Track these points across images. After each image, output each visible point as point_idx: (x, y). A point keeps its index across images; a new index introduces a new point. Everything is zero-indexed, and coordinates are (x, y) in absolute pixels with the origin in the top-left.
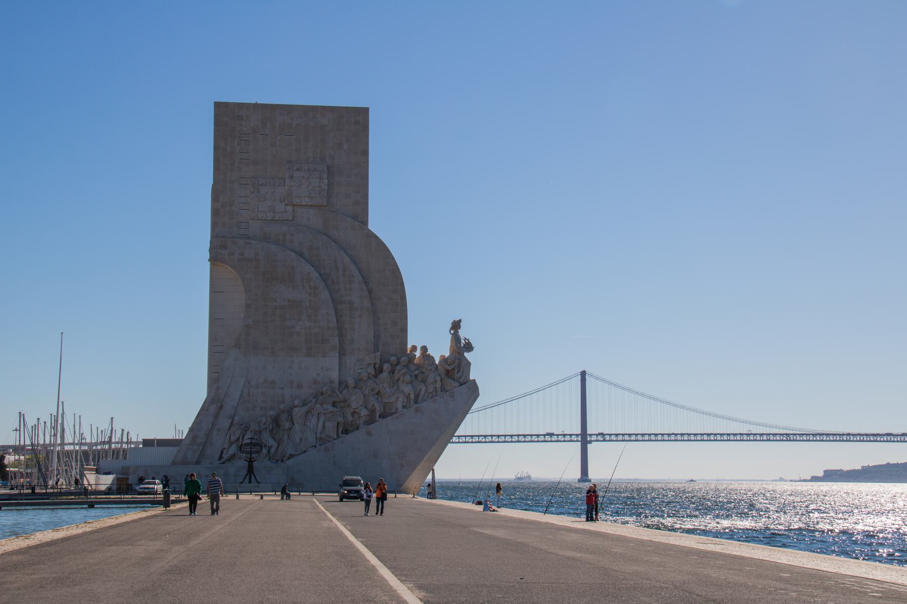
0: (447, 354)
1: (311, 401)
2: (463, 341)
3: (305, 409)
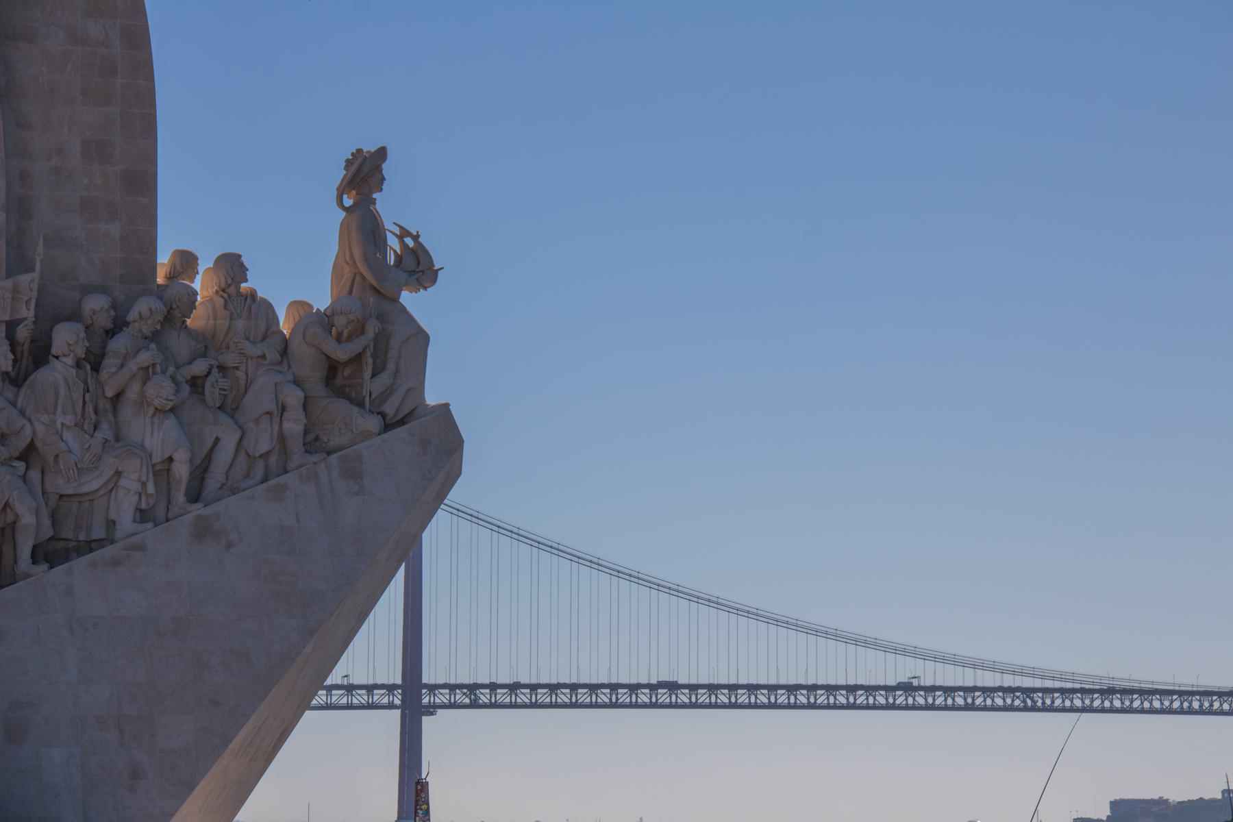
2: (393, 243)
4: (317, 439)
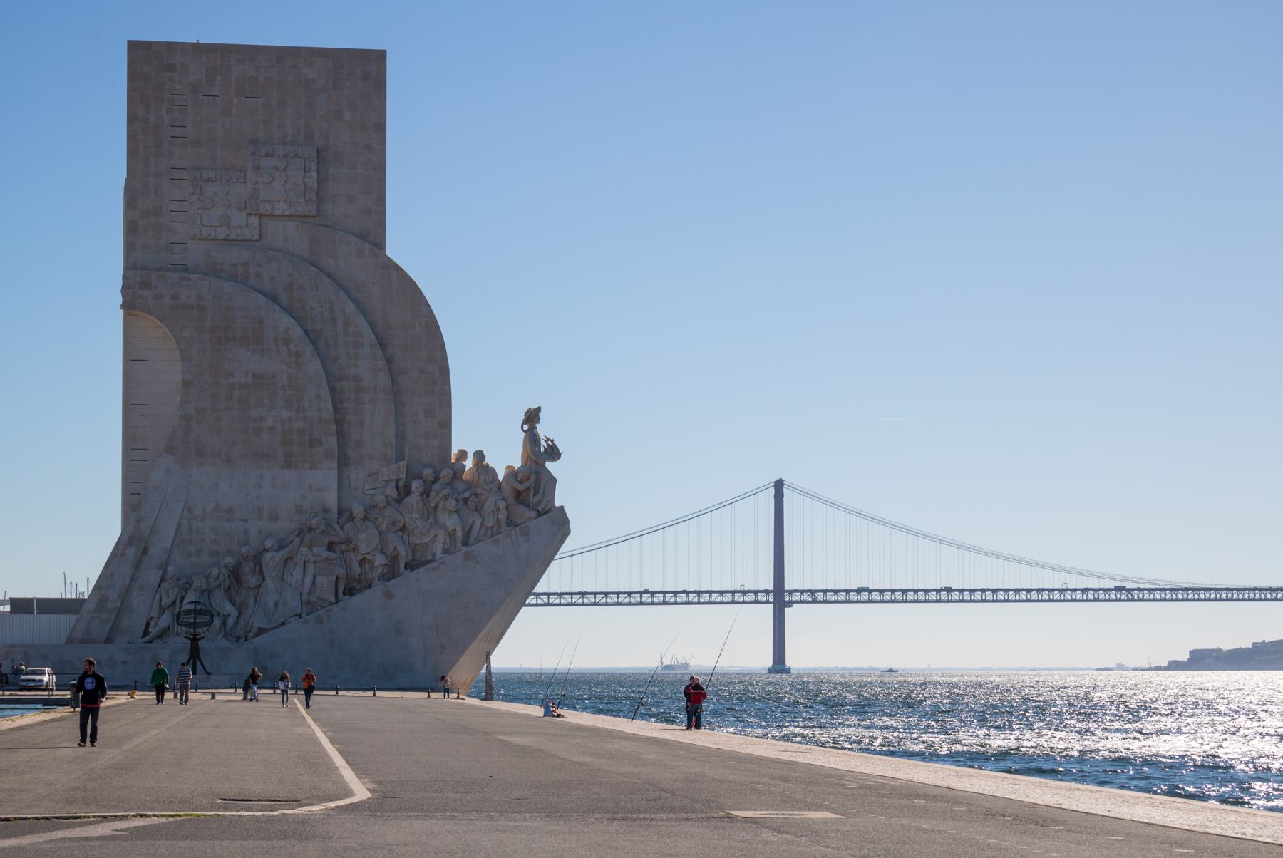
0: (517, 464)
1: (292, 542)
2: (543, 443)
3: (282, 554)
4: (512, 521)
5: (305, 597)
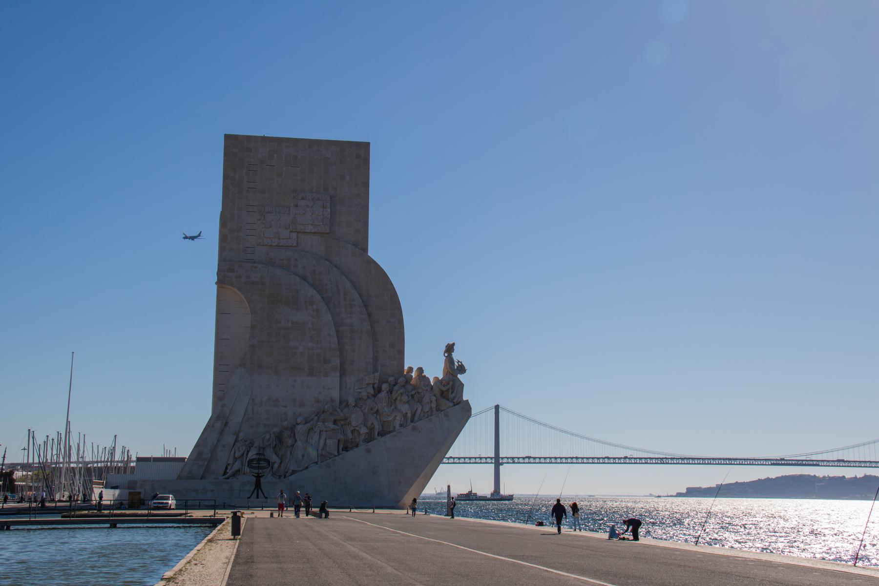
0: (441, 377)
2: (456, 364)
3: (308, 426)
4: (439, 408)
5: (320, 452)
